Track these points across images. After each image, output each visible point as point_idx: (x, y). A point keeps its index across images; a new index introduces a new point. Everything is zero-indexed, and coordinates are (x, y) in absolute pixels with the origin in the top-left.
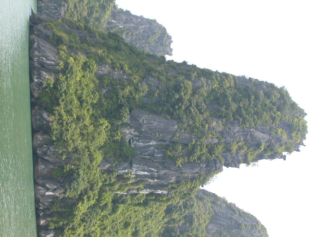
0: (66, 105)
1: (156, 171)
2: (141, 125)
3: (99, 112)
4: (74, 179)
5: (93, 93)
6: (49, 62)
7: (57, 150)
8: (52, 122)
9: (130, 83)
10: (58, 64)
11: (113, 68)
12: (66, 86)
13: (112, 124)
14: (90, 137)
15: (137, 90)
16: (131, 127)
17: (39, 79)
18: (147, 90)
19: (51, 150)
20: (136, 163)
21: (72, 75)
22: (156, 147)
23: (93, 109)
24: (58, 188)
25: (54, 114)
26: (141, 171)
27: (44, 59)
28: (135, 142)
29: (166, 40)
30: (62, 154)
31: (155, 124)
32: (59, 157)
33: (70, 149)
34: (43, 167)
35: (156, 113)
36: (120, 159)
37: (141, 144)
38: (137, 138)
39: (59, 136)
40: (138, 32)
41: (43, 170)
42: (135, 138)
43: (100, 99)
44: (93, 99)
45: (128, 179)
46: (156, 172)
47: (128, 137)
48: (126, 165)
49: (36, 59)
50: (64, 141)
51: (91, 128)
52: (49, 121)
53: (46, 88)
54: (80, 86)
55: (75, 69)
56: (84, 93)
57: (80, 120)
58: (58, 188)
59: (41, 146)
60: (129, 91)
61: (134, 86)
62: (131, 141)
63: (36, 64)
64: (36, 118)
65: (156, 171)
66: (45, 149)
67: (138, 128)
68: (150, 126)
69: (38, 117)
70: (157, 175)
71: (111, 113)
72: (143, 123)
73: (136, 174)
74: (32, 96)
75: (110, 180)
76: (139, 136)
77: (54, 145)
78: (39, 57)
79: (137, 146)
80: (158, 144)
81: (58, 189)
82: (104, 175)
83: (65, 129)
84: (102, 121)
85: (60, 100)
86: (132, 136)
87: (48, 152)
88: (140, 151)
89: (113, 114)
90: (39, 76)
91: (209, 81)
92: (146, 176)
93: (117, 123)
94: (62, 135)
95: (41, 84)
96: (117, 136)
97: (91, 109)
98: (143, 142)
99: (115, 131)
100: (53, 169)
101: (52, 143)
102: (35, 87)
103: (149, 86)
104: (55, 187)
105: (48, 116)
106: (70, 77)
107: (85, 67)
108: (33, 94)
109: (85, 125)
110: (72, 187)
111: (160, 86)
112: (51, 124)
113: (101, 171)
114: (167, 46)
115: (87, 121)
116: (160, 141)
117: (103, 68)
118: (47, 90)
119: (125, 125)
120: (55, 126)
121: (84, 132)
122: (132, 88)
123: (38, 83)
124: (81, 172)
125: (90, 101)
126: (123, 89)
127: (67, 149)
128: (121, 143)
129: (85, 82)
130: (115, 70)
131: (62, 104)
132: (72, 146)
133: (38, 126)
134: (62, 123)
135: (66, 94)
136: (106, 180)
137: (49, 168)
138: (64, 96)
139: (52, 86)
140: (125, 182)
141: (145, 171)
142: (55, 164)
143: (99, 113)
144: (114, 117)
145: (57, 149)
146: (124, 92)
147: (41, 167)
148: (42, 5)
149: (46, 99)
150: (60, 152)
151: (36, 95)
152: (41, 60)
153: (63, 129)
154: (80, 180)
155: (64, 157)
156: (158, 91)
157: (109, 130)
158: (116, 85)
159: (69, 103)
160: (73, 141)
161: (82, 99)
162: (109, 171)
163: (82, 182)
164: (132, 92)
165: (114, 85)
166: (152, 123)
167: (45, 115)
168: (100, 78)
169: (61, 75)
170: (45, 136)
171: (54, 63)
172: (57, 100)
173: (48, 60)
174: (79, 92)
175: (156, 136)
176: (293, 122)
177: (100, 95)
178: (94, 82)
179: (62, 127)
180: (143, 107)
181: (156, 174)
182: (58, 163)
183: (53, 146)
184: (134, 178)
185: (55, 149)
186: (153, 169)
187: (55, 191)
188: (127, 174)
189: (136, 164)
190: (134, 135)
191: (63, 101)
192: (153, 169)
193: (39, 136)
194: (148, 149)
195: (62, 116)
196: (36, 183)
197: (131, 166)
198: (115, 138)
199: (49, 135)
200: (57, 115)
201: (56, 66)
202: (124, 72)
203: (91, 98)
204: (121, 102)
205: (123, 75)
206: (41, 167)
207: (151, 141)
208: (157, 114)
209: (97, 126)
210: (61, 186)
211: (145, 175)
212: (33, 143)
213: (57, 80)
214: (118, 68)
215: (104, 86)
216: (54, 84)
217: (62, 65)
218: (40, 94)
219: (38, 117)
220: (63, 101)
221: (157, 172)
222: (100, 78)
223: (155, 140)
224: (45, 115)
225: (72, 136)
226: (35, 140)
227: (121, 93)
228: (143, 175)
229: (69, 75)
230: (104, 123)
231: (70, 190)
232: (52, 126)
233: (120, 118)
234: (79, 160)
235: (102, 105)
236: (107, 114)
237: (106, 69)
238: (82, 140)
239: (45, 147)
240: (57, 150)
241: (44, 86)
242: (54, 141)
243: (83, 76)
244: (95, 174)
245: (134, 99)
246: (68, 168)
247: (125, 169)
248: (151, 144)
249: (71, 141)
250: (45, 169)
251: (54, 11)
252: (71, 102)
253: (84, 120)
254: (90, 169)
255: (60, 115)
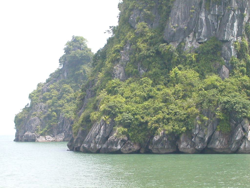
0: (148, 115)
1: (233, 12)
2: (180, 30)
3: (162, 77)
4: (232, 108)
5: (141, 84)
6: (102, 131)
7: (198, 126)
8: (165, 130)
9: (133, 42)
10: (104, 122)
11: (118, 60)
12: (128, 113)
13: (178, 63)
14: (188, 88)
15: (142, 34)
16: (183, 41)
17: (117, 142)
18: (143, 23)
19: (197, 132)
20: (222, 35)
21: (116, 107)
22: (208, 12)
23: (159, 84)
24: (242, 126)
25: (156, 128)
26: (233, 29)
27: (97, 137)
28: (201, 37)
30: (202, 121)
31: (179, 13)
32: (206, 124)
33: (197, 111)
34: (217, 143)
35: (168, 14)
36: (219, 54)
37: (203, 30)
38: (197, 34)
39: (182, 124)
41: (221, 143)
42: (197, 37)
43: (149, 76)
44: (148, 84)
45: (242, 45)
46: (234, 13)
47: (196, 45)
48: (225, 48)
49: (98, 146)
50: (188, 117)
51: (178, 87)
52: (164, 133)
53: (128, 136)
54: (132, 98)
55: (111, 103)
56: (139, 93)
57: (167, 99)
58: (242, 126)
59: (194, 144)
60: (143, 43)
61: (138, 38)
62: (200, 41)
64: (161, 148)
65: (233, 12)
66: (197, 140)
67: (186, 33)
68: (181, 19)
69: (160, 146)
70: (238, 11)
71: (165, 63)
72: (177, 27)
73: (238, 36)
74: (138, 152)
75: (242, 66)
76: (195, 33)
77: (191, 130)
78: (96, 143)
79: (205, 35)
80: (204, 10)
81: (244, 126)
82: (236, 73)
83: (174, 115)
84: (172, 74)
85: (142, 120)
86: (195, 41)
87: (200, 136)
88: (212, 31)
89: (166, 61)
90: (114, 143)
92: (240, 25)
93: (176, 58)
94: (181, 119)
95: (123, 141)
96: (192, 58)
97: (158, 86)
98: (202, 28)
99: (186, 60)
100: (220, 131)
101: (189, 132)
102: (127, 148)
103: (139, 20)
104: (239, 129)
105: (157, 134)
106: (119, 109)
107: (112, 92)
108: (135, 150)
109: (174, 94)
110: (240, 110)
111: (139, 8)
112: (167, 132)
113: (230, 76)
115: (169, 91)
116: (201, 8)
117: (117, 72)
118: (130, 134)
119: (180, 49)
120: (169, 128)
121: (181, 94)
122: (139, 40)
123: (122, 144)
124: (225, 99)
125: (150, 87)
126: (140, 51)
127: (196, 114)
128: (200, 53)
129: (128, 93)
130: (118, 59)
131: (147, 118)
132: (194, 108)
133: (170, 147)
134: (168, 119)
135: (136, 114)
136: (242, 71)
137: (219, 135)
138: (138, 116)
139: (126, 130)
140: (246, 49)
141: (232, 26)
142: (215, 129)
143: (164, 77)
144: (169, 60)
145: (196, 126)
146: (144, 49)
147: (217, 144)
149: (140, 137)
150: (199, 122)
151: (136, 147)
152: (99, 140)
153: (173, 118)
154: (233, 100)
155: (205, 118)
156: (145, 10)
157: (184, 66)
158: (135, 57)
159: (146, 110)
160: (189, 107)
161: (146, 96)
162: (232, 67)
163: (236, 98)
164: (145, 40)
165: (135, 61)
166: (178, 18)
167: (156, 138)
168: (127, 75)
169: (116, 119)
170: (182, 139)
171: (102, 127)
172: (141, 124)
173: (99, 132)
174: (138, 99)
175: (194, 12)
177: (145, 76)
178: (130, 82)
179: (172, 120)
180: (162, 28)
181: (236, 13)
182: (213, 125)
183: (193, 130)
184: (242, 38)
185: (196, 128)
186: (231, 16)
187: (246, 130)
188: (236, 46)
189: (224, 35)
190: (193, 38)
191: (143, 118)
192: (231, 16)
193: (182, 146)
194: (210, 22)
195: (159, 119)
196: (237, 152)
197: (227, 41)
198: (194, 59)
199: (180, 134)
200: (157, 125)
201: (106, 124)
202: (122, 48)
203: (146, 86)
204: (154, 52)
205: (126, 49)
206: (217, 144)
207: (201, 19)
208: (170, 12)
209: (177, 80)
210: (240, 122)
211: (238, 26)
212: (190, 152)
213: (121, 123)
214: (118, 55)
215: (135, 72)
216: (125, 127)
217: (105, 118)
218: (135, 143)
219: (160, 146)
220: (143, 118)
221: (234, 11)
222: (127, 75)
223: (199, 13)
224: (156, 138)
225: (183, 109)
226: (186, 151)
227: (144, 52)
228: (238, 28)
229: (117, 109)
230: (174, 72)
231: (245, 112)
232: (168, 130)
233: (171, 54)
234: (210, 101)
235: (156, 74)
236: (166, 68)
237: (118, 69)
238: (190, 97)
239: (195, 140)
240: (198, 126)
241: (126, 138)
242: (187, 128)
243: (122, 95)
244: (232, 83)
245: (151, 38)
246: (219, 114)
247: (230, 49)
248: (204, 19)
249: (189, 110)
250: (220, 141)
252: (146, 108)
253: (167, 95)
254: (224, 89)
255: (157, 121)
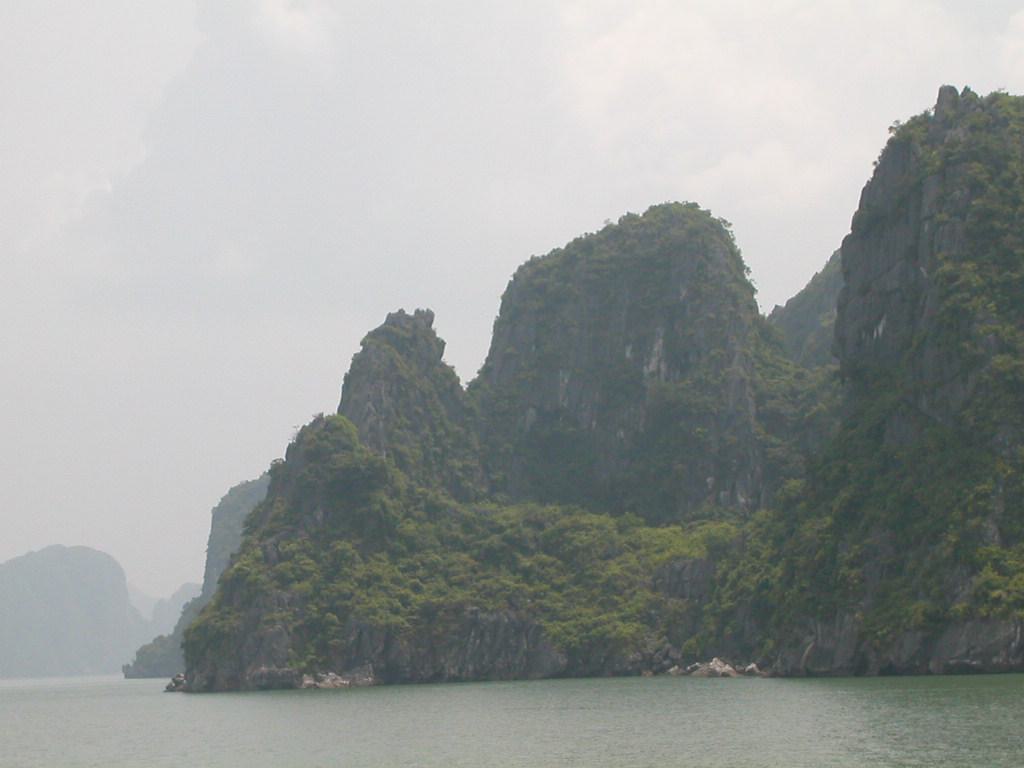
11: (985, 513)
27: (1013, 645)
29: (404, 328)
40: (393, 410)
49: (1012, 662)
63: (1019, 660)
91: (980, 316)
114: (415, 327)
148: (471, 668)
168: (1007, 541)
173: (1015, 637)
176: (1019, 132)
222: (1007, 541)
237: (991, 528)
251: (488, 639)
